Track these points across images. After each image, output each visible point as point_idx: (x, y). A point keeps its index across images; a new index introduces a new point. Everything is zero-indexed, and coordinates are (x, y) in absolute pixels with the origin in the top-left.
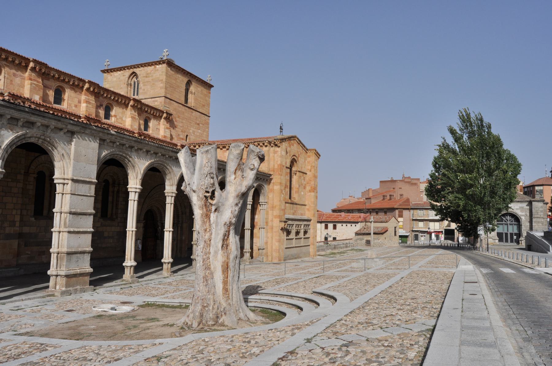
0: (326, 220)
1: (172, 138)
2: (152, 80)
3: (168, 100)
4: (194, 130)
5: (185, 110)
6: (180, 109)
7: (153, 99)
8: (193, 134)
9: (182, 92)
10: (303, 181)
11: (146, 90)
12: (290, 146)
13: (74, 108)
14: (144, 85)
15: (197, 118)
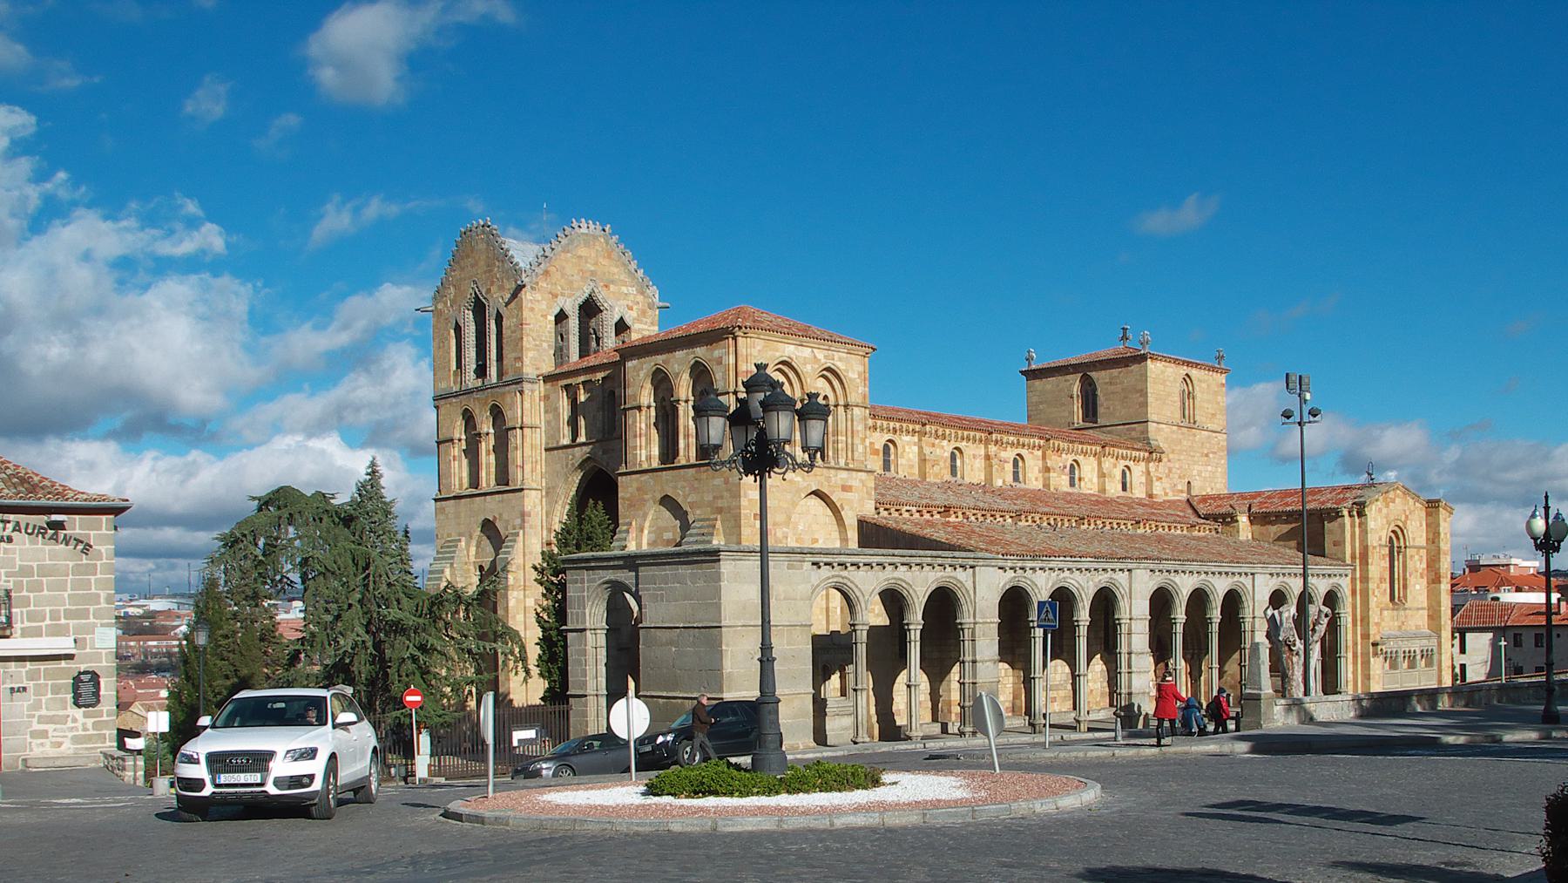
0: (1518, 621)
1: (1166, 494)
2: (1123, 389)
3: (1155, 424)
4: (1200, 468)
5: (1183, 434)
6: (1175, 436)
7: (1127, 426)
8: (1197, 477)
9: (1175, 402)
10: (1418, 563)
11: (1111, 408)
12: (1387, 506)
13: (1034, 483)
14: (1106, 399)
15: (1203, 444)
